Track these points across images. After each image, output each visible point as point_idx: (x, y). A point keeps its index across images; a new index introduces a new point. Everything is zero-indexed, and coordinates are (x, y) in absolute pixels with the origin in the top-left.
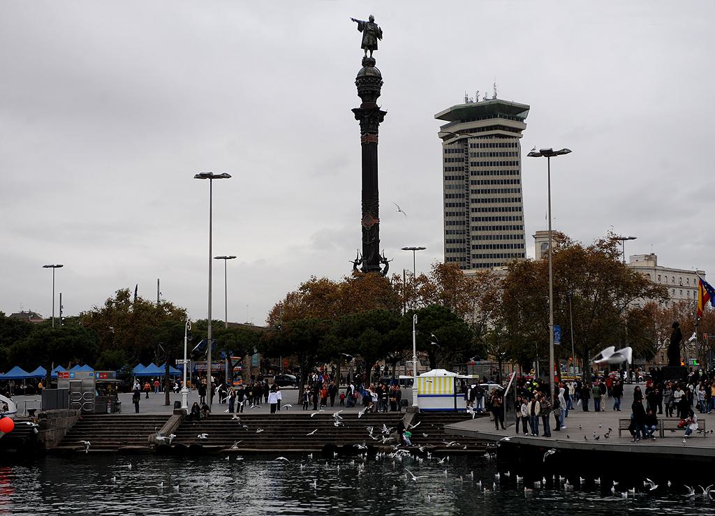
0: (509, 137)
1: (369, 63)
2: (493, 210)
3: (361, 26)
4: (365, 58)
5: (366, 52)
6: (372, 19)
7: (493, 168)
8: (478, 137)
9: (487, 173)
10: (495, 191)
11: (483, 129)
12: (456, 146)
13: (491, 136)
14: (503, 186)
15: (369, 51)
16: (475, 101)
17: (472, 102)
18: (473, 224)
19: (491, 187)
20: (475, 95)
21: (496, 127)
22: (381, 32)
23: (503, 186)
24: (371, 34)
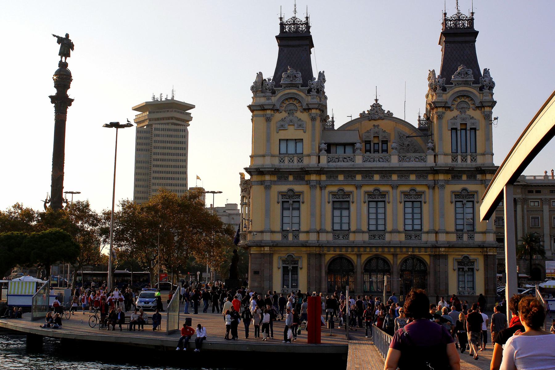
0: (180, 125)
1: (63, 66)
3: (60, 40)
4: (61, 62)
5: (62, 58)
6: (67, 35)
8: (159, 124)
10: (169, 160)
11: (163, 119)
13: (168, 124)
14: (175, 157)
15: (64, 58)
18: (153, 181)
19: (166, 157)
20: (159, 96)
21: (172, 118)
22: (73, 45)
23: (175, 157)
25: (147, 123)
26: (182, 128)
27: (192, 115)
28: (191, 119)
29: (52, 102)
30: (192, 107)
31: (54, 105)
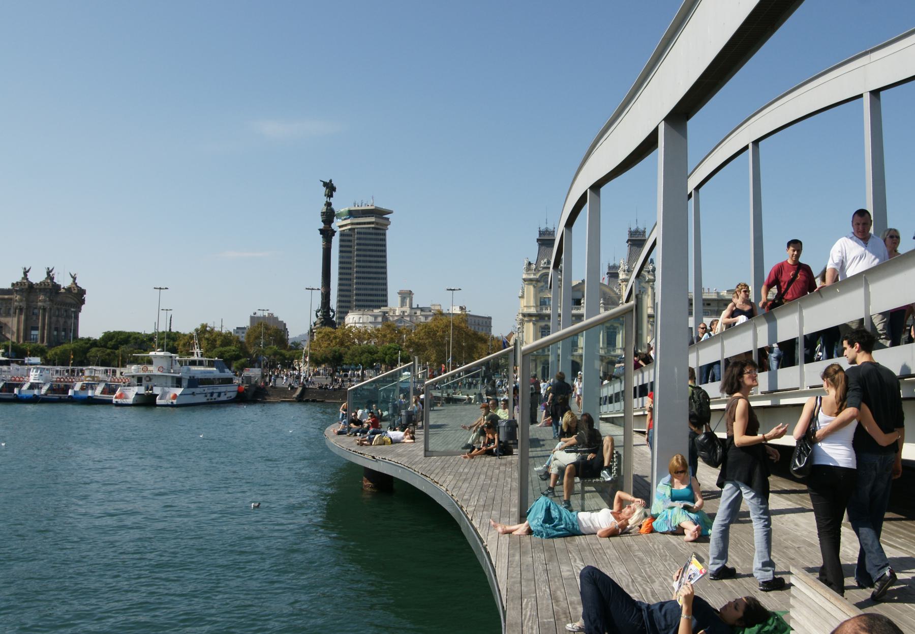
1: (329, 204)
2: (369, 273)
3: (326, 185)
4: (327, 202)
6: (331, 181)
14: (376, 259)
23: (376, 259)
24: (330, 188)
25: (349, 227)
26: (381, 232)
27: (390, 220)
28: (389, 223)
29: (321, 234)
30: (390, 212)
31: (321, 236)
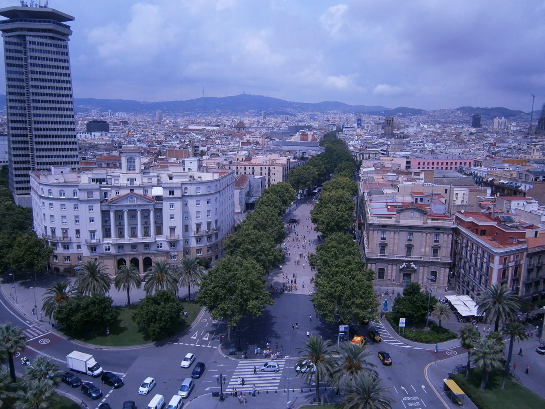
7: (48, 63)
8: (33, 36)
9: (43, 66)
10: (51, 81)
11: (39, 30)
12: (15, 40)
13: (45, 37)
14: (57, 78)
16: (29, 6)
17: (27, 6)
19: (47, 77)
21: (50, 31)
23: (57, 78)
26: (62, 43)
27: (71, 29)
28: (71, 33)
